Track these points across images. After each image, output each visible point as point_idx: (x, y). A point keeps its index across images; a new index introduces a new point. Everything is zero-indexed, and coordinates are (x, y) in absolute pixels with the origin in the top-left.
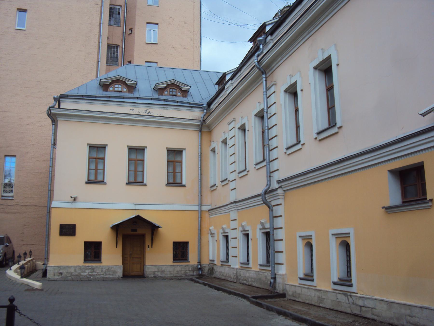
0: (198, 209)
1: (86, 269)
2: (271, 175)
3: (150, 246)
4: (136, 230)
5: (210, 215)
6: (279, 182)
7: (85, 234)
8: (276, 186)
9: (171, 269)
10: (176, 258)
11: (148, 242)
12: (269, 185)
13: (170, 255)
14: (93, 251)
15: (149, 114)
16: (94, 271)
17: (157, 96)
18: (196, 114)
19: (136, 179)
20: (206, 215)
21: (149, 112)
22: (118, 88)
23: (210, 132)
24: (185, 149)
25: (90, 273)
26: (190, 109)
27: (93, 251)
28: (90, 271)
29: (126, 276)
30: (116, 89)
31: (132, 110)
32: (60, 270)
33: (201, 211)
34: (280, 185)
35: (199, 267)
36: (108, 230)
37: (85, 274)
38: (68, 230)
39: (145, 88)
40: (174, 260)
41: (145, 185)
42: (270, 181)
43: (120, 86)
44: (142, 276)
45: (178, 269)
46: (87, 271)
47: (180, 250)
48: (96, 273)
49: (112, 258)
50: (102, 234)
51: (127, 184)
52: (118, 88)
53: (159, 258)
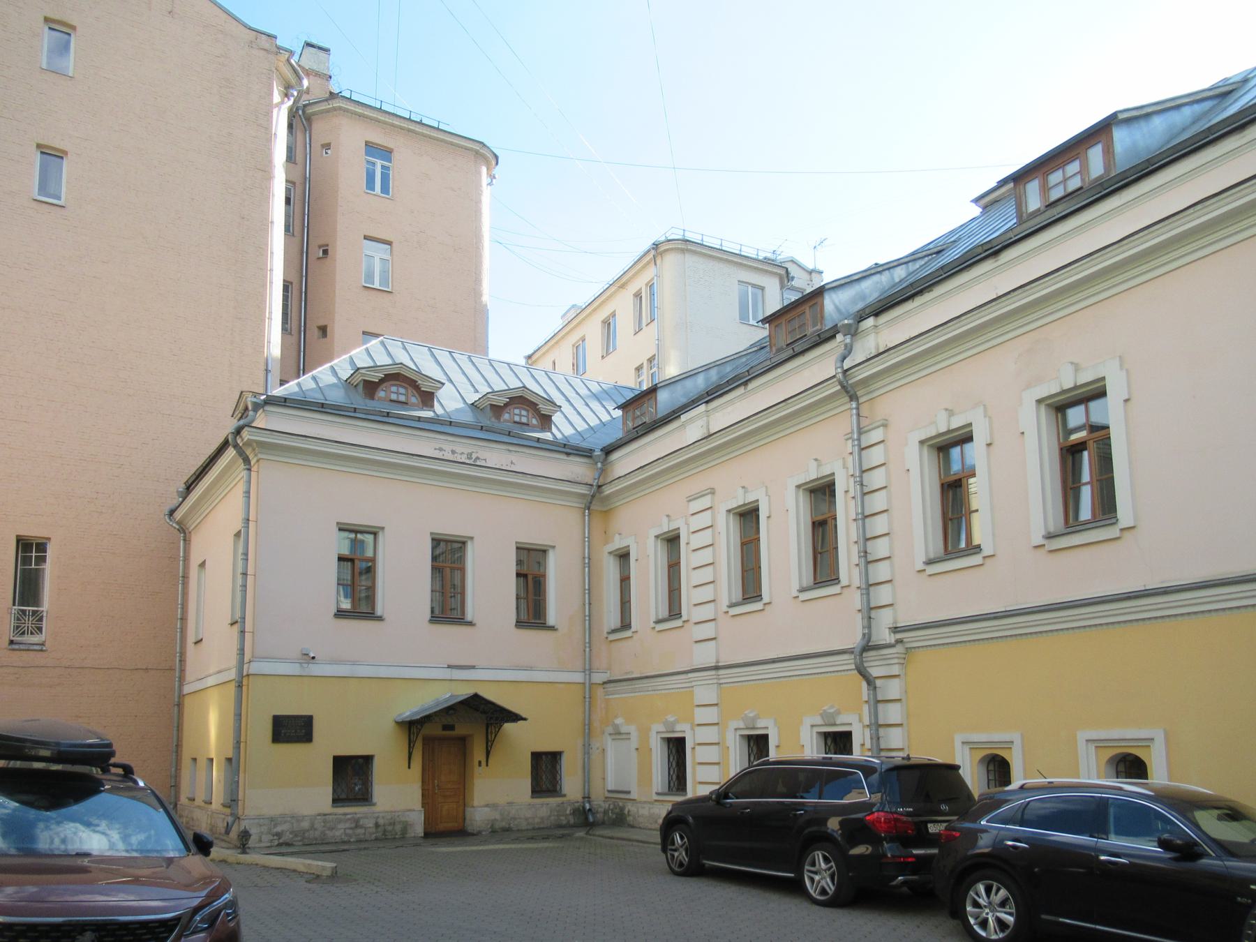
0: (581, 681)
1: (340, 821)
2: (873, 614)
3: (484, 763)
4: (451, 728)
5: (607, 694)
6: (895, 630)
7: (334, 739)
8: (889, 638)
9: (529, 814)
10: (537, 791)
11: (478, 753)
12: (867, 637)
13: (526, 784)
14: (352, 774)
15: (478, 463)
16: (357, 827)
17: (486, 422)
18: (577, 469)
19: (448, 607)
20: (600, 692)
21: (477, 458)
22: (520, 415)
23: (607, 513)
24: (472, 538)
25: (349, 831)
26: (565, 457)
27: (352, 774)
28: (348, 825)
29: (431, 834)
30: (394, 397)
31: (441, 449)
32: (275, 825)
33: (591, 684)
34: (899, 636)
35: (588, 807)
36: (388, 726)
37: (338, 833)
38: (293, 729)
39: (449, 402)
40: (533, 792)
41: (380, 619)
42: (869, 627)
43: (402, 390)
44: (460, 833)
45: (544, 812)
46: (341, 826)
47: (545, 768)
48: (362, 831)
49: (398, 792)
50: (374, 736)
51: (431, 621)
52: (520, 415)
53: (499, 789)
